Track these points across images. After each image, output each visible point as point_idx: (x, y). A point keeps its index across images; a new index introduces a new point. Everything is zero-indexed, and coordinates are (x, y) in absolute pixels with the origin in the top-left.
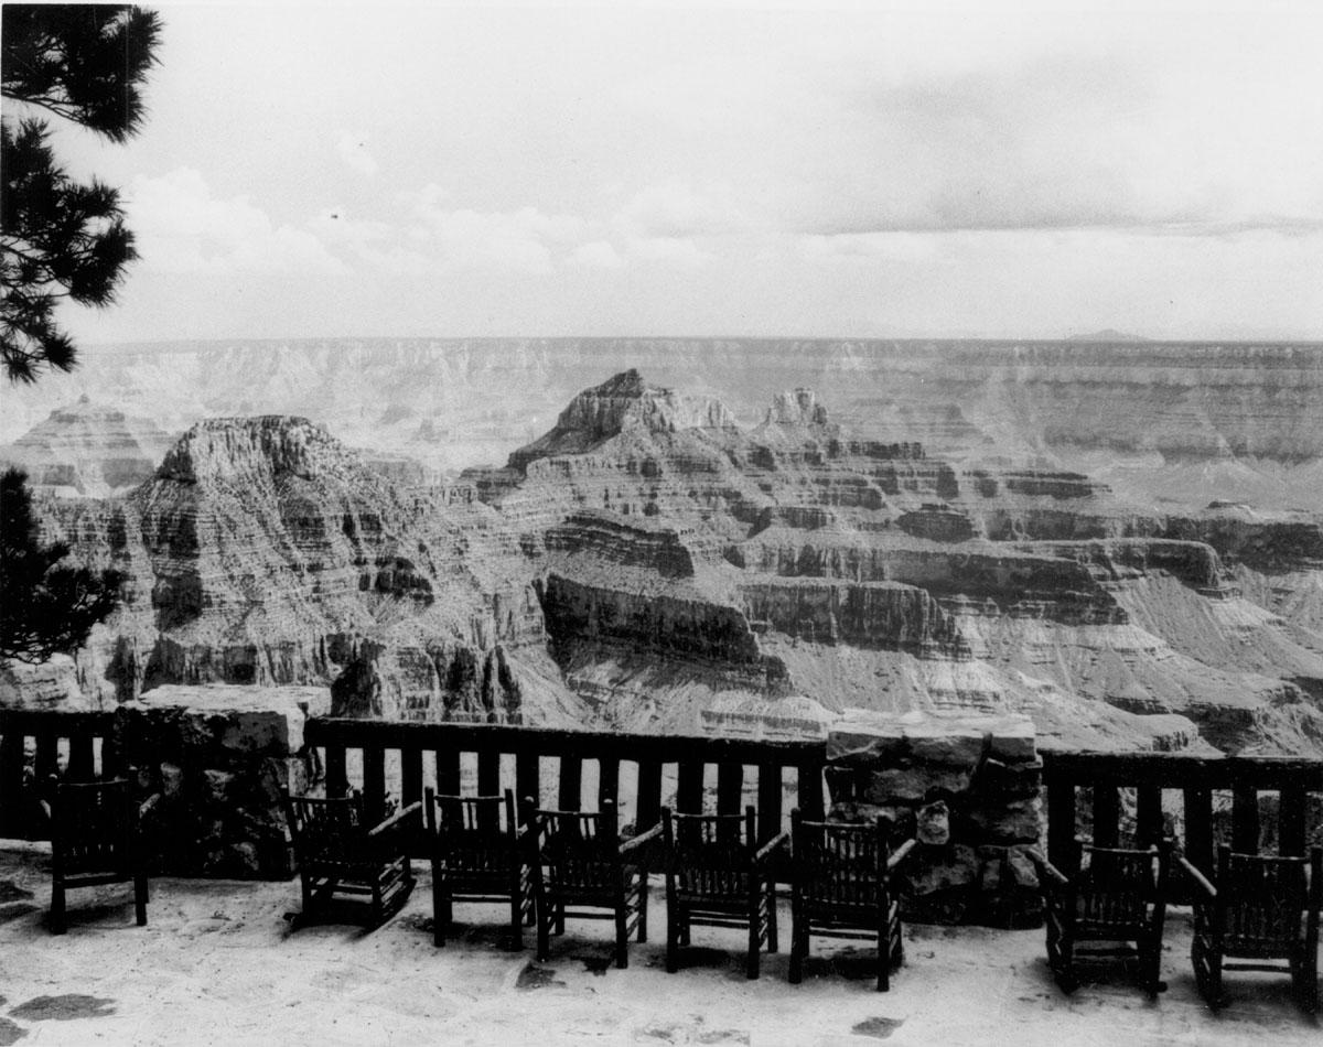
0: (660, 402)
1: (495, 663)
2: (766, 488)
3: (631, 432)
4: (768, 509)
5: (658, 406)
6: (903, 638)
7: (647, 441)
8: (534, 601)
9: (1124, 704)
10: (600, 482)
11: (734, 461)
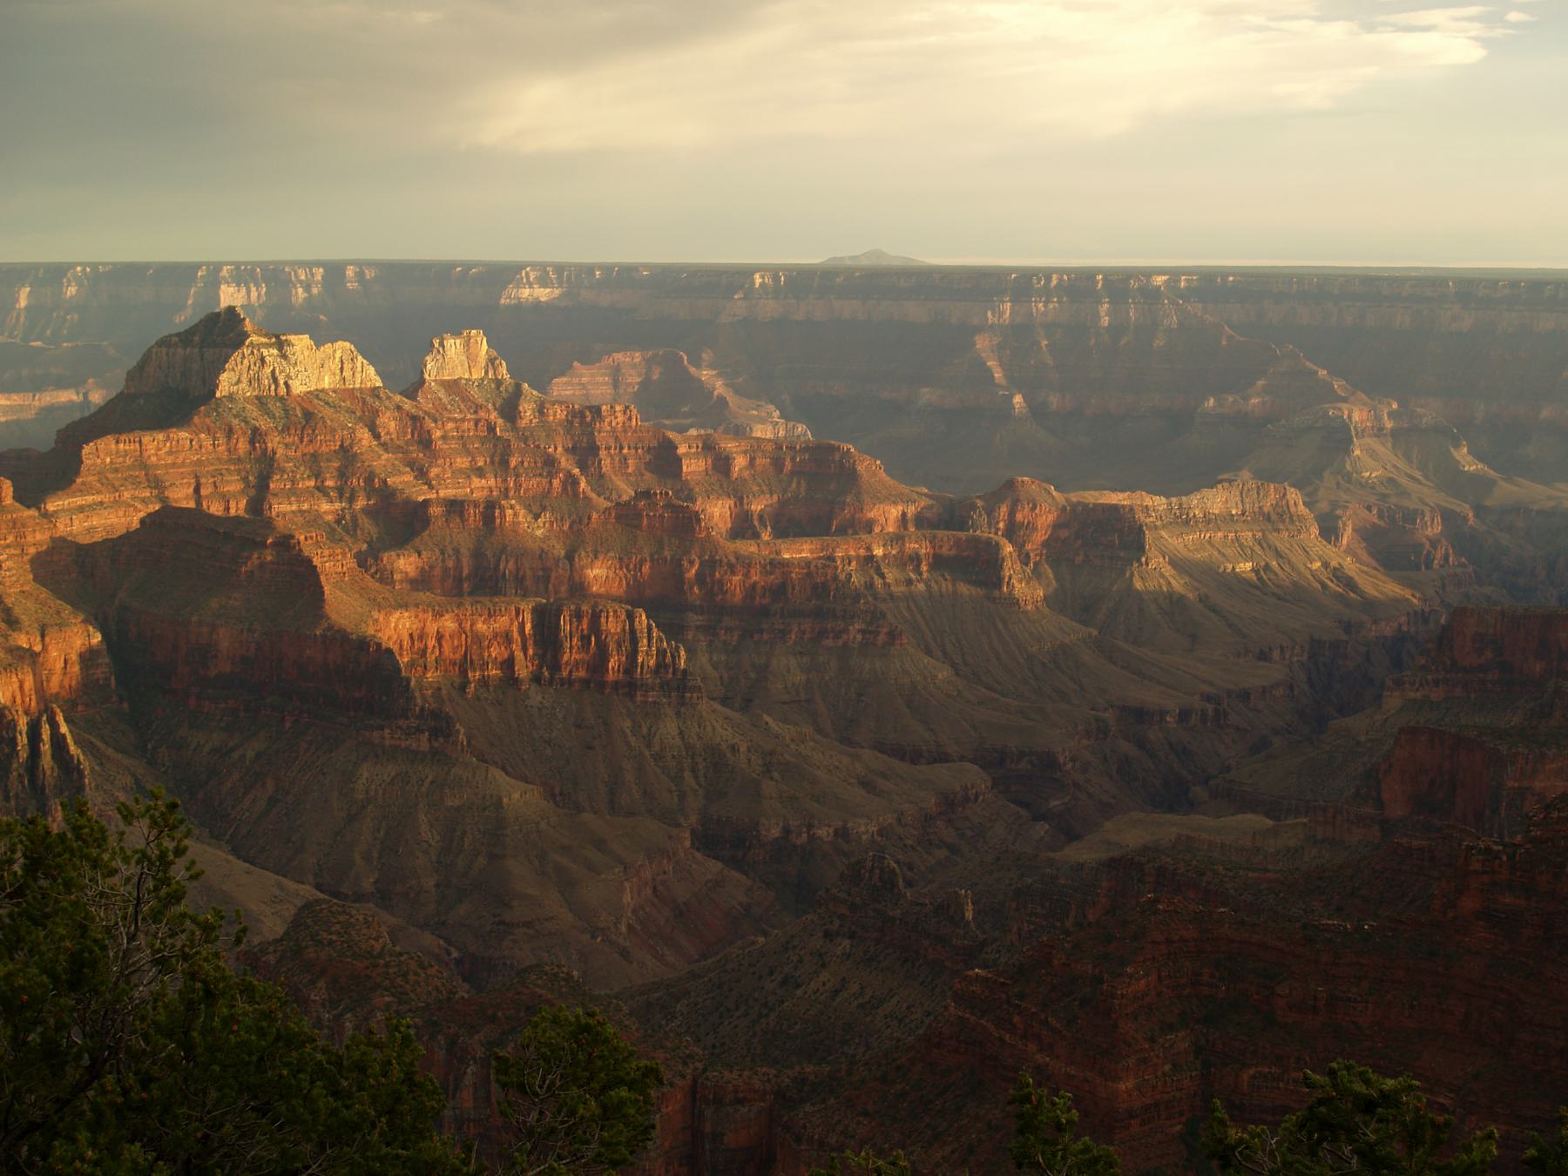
0: (271, 354)
2: (422, 474)
3: (231, 397)
4: (426, 503)
5: (268, 359)
6: (611, 676)
7: (253, 411)
8: (97, 638)
9: (899, 752)
10: (182, 466)
11: (377, 436)
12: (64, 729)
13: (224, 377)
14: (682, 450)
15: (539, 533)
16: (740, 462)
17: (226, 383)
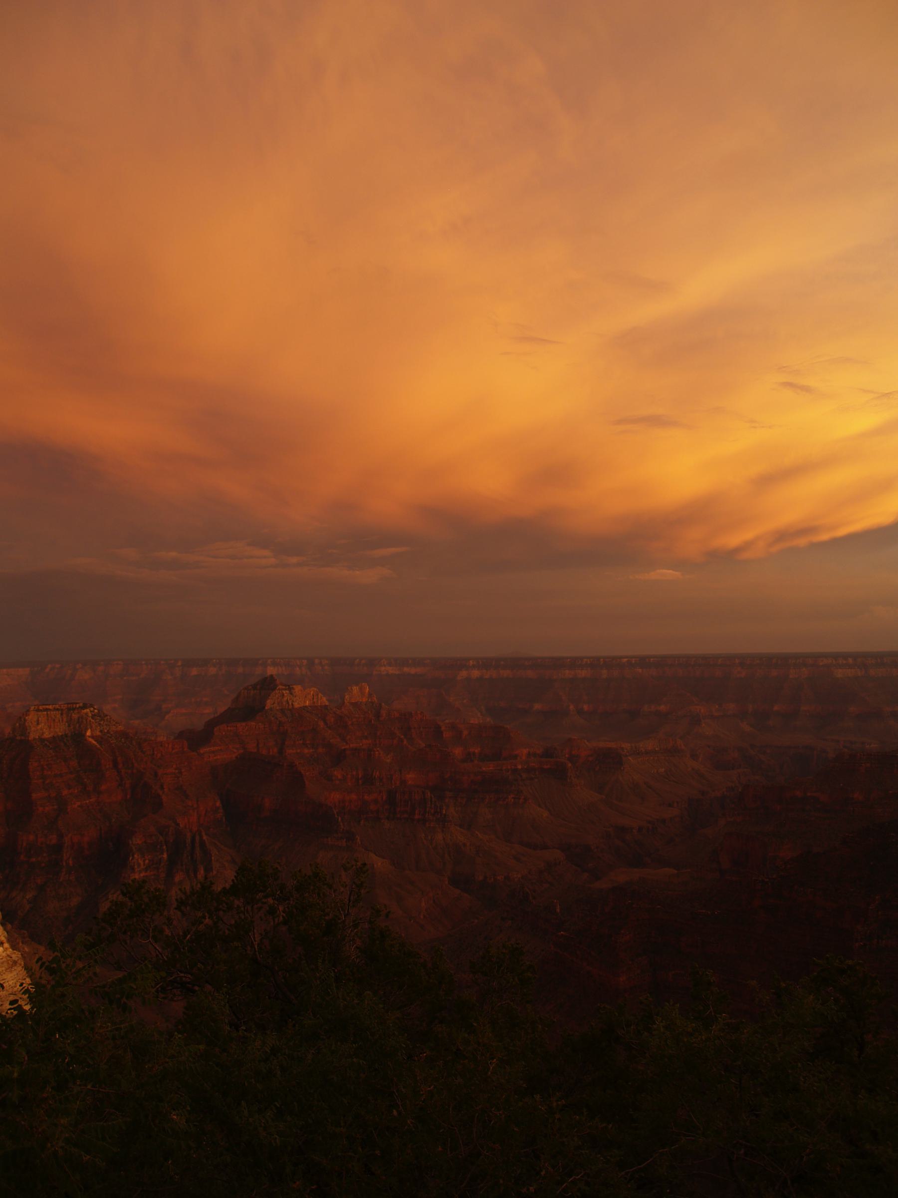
1: (197, 838)
3: (271, 709)
6: (417, 817)
8: (218, 804)
12: (205, 838)
13: (268, 701)
14: (443, 728)
15: (388, 761)
16: (465, 733)
17: (269, 704)
